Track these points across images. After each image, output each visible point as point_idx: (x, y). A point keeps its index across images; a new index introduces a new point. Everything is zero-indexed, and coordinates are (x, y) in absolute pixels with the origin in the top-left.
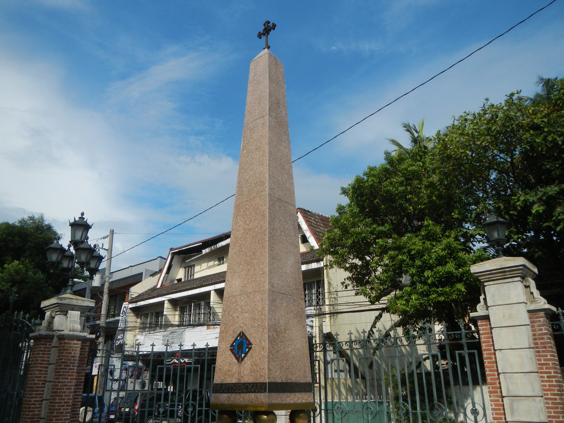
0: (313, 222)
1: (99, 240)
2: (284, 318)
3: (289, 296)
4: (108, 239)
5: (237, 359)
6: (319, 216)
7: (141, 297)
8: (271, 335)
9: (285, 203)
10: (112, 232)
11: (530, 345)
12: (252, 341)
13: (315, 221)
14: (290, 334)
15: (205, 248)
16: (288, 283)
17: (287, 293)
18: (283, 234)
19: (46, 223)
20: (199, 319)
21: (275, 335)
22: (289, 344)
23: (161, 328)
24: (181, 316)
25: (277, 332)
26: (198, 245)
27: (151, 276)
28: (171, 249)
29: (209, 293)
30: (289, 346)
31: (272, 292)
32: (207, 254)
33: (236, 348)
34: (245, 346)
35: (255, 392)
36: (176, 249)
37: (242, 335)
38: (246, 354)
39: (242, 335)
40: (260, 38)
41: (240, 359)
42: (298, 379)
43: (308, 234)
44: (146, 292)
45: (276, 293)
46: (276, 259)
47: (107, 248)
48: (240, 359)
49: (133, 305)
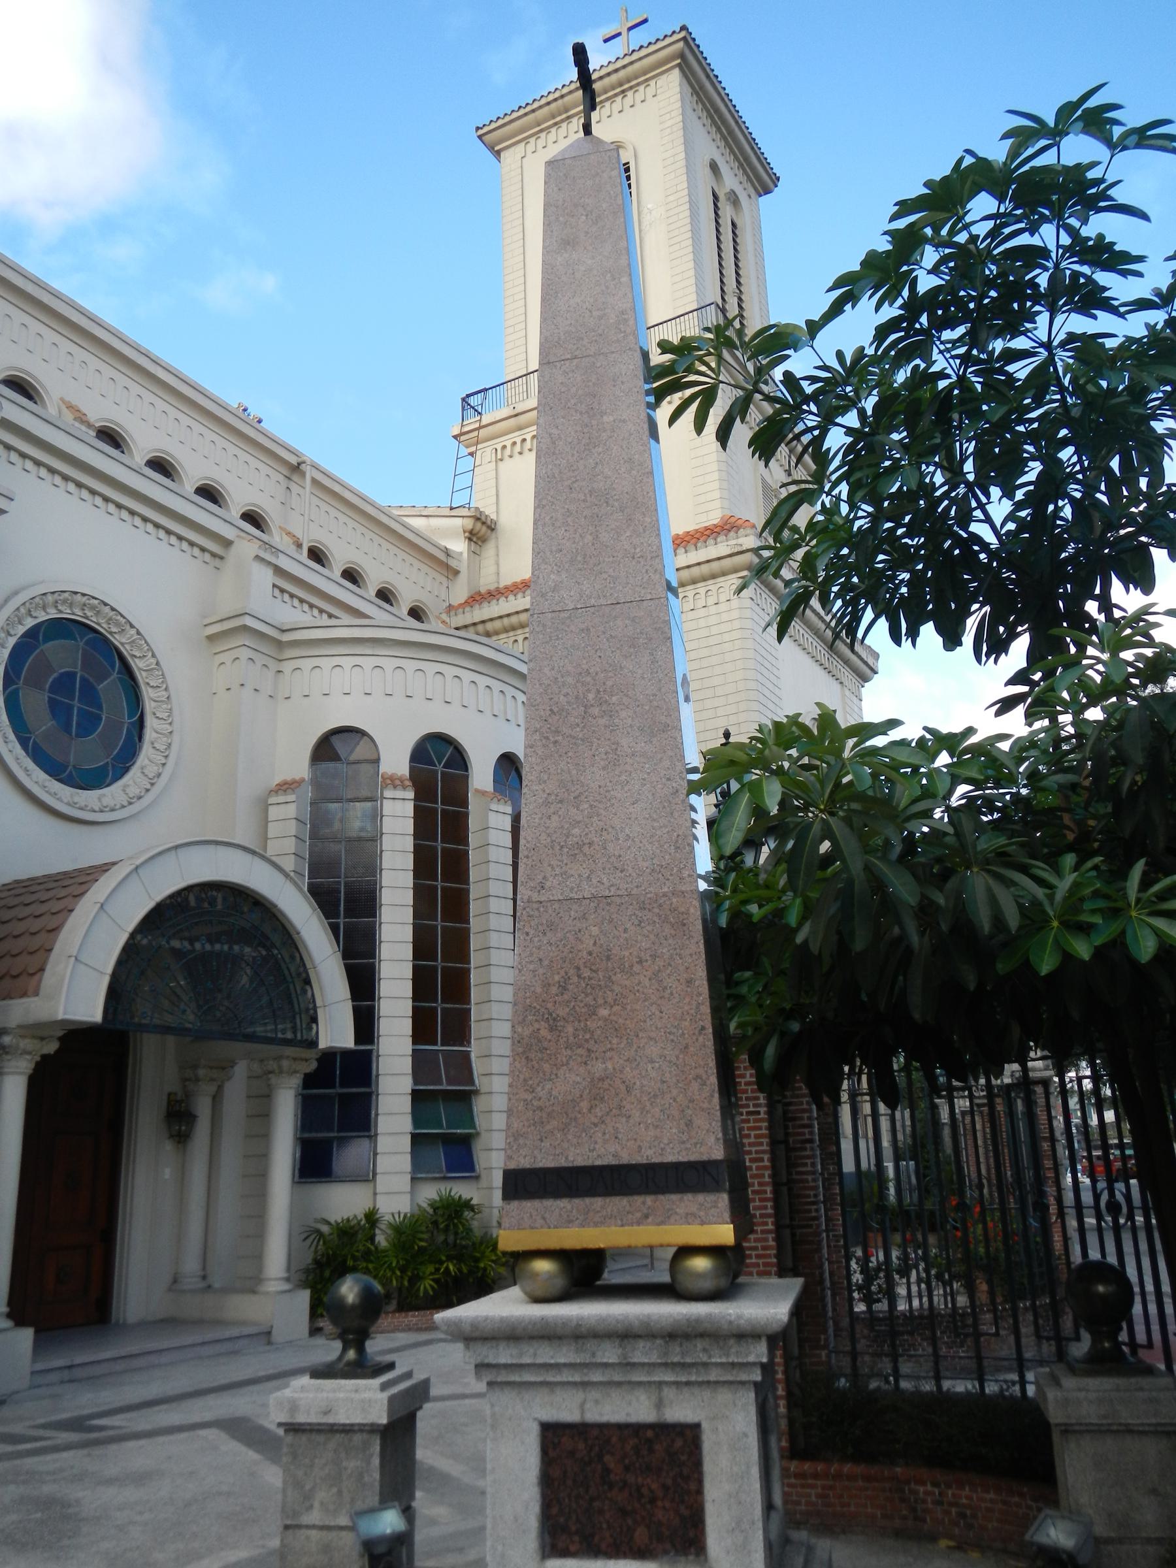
2: (586, 973)
3: (618, 900)
8: (527, 1032)
9: (607, 609)
14: (614, 1018)
16: (613, 859)
17: (607, 893)
18: (596, 711)
21: (544, 1032)
22: (612, 1049)
25: (554, 1020)
30: (609, 1054)
31: (535, 906)
42: (650, 1152)
45: (556, 906)
46: (561, 802)
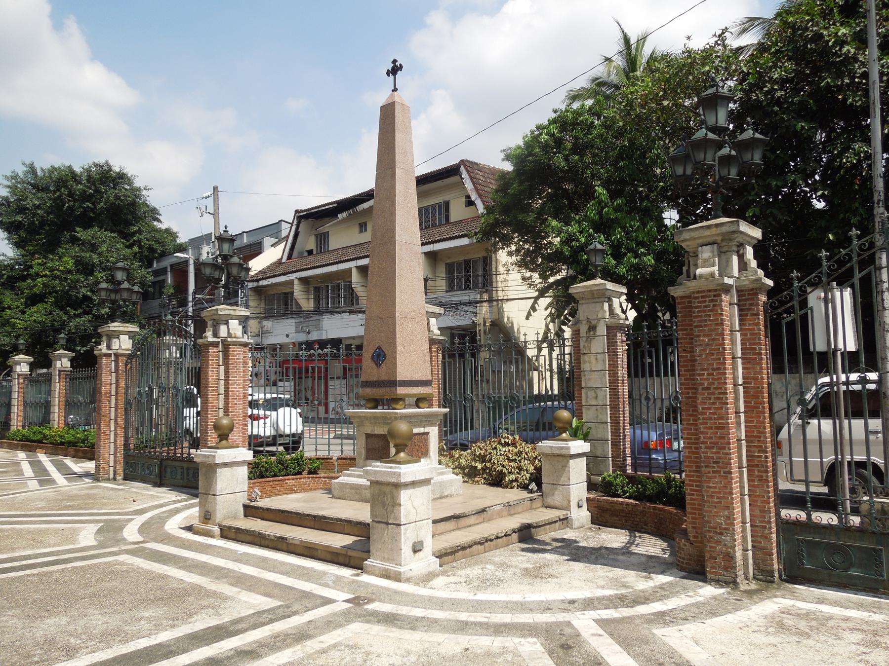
0: (481, 178)
1: (199, 201)
4: (212, 199)
5: (377, 365)
6: (489, 169)
7: (265, 274)
10: (215, 189)
11: (604, 350)
12: (386, 352)
13: (483, 176)
15: (341, 212)
19: (116, 169)
20: (339, 302)
23: (291, 314)
24: (317, 300)
26: (331, 206)
27: (272, 246)
28: (297, 212)
29: (350, 270)
32: (344, 220)
33: (376, 357)
34: (382, 356)
35: (389, 386)
36: (302, 211)
37: (379, 348)
38: (383, 361)
39: (379, 348)
40: (389, 76)
41: (378, 366)
43: (474, 197)
44: (268, 267)
47: (212, 212)
48: (378, 366)
49: (255, 284)
